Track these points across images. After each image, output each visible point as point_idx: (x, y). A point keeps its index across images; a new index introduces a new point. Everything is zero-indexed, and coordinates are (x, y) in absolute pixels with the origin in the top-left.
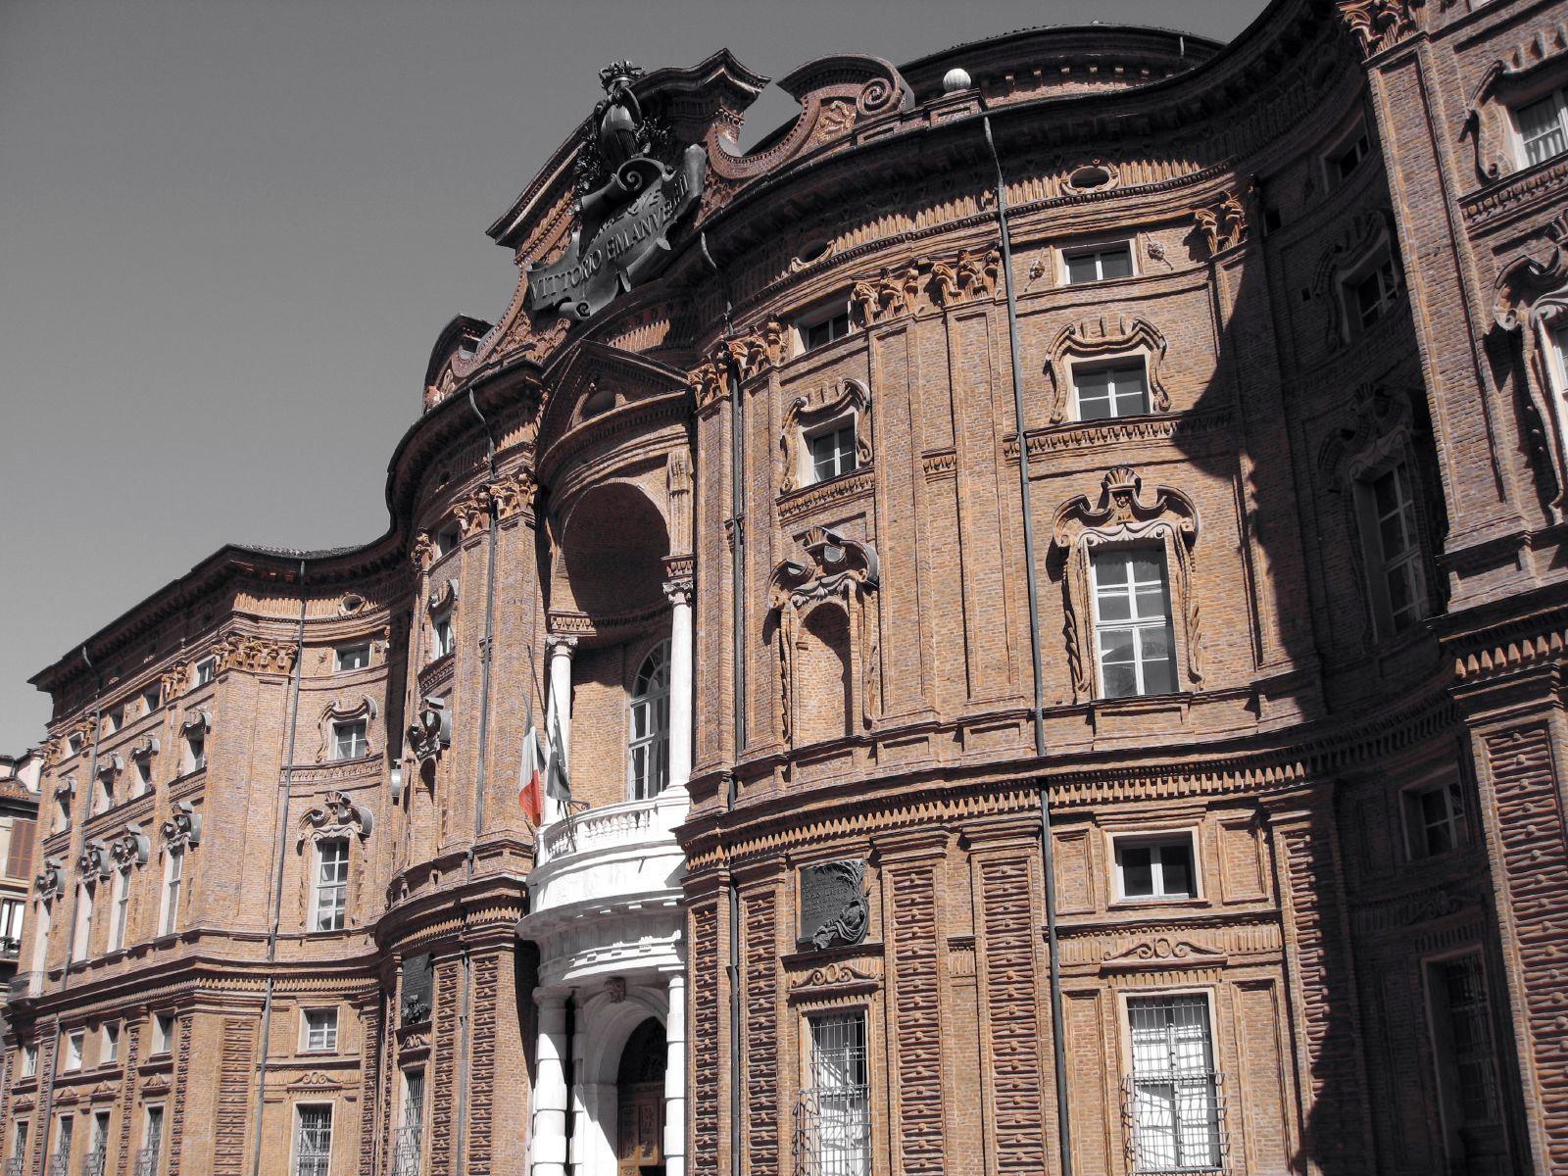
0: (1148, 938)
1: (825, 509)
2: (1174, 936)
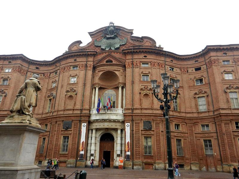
0: (178, 133)
1: (146, 84)
2: (180, 134)
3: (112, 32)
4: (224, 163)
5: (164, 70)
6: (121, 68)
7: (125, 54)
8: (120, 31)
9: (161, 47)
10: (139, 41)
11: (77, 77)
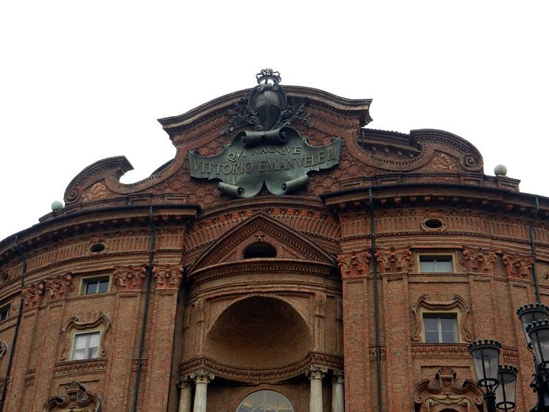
1: (442, 358)
3: (270, 115)
5: (531, 289)
6: (320, 281)
7: (335, 212)
8: (310, 111)
9: (510, 175)
10: (402, 150)
11: (101, 329)
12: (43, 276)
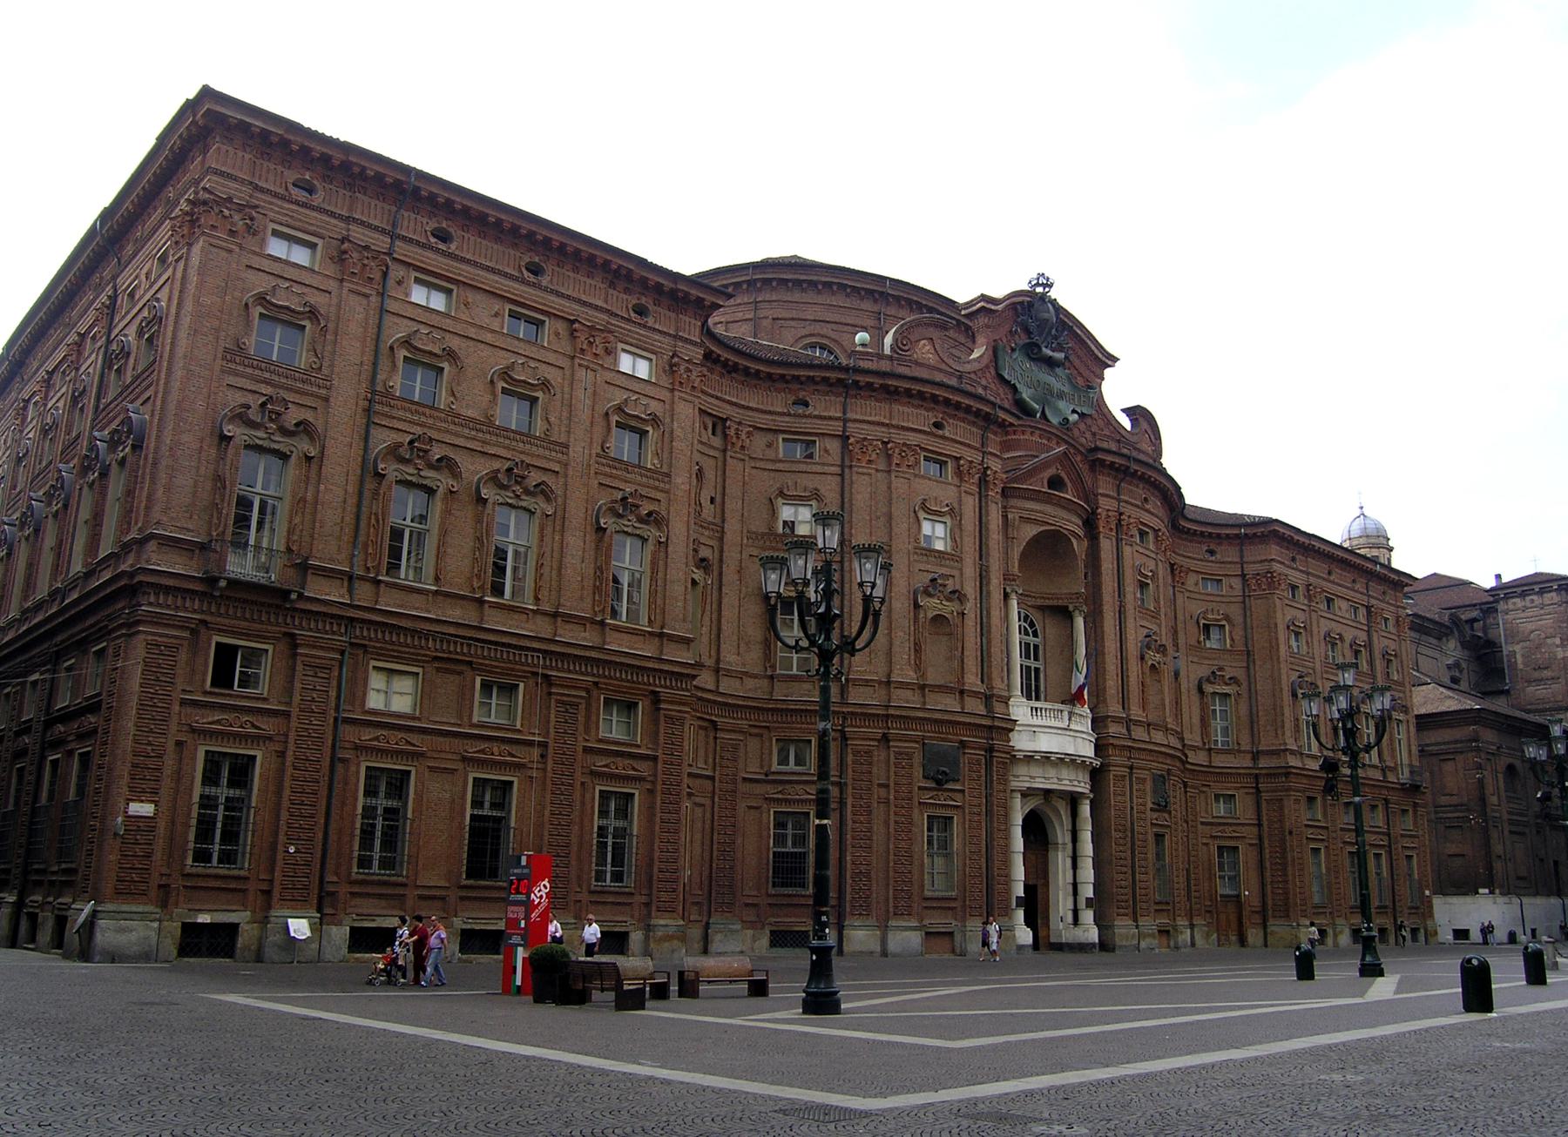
4: (1271, 922)
7: (1096, 465)
12: (881, 432)
